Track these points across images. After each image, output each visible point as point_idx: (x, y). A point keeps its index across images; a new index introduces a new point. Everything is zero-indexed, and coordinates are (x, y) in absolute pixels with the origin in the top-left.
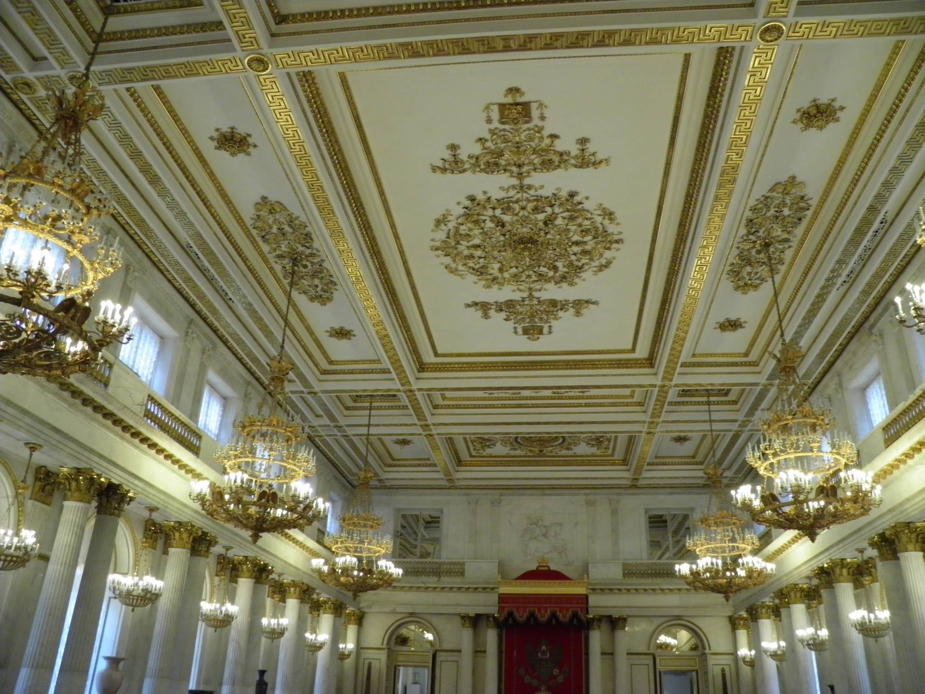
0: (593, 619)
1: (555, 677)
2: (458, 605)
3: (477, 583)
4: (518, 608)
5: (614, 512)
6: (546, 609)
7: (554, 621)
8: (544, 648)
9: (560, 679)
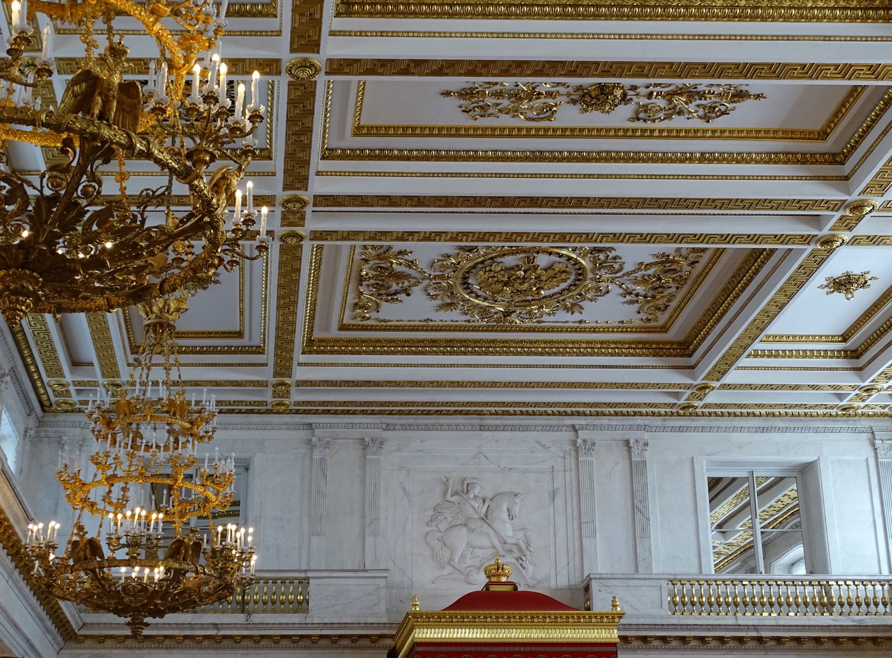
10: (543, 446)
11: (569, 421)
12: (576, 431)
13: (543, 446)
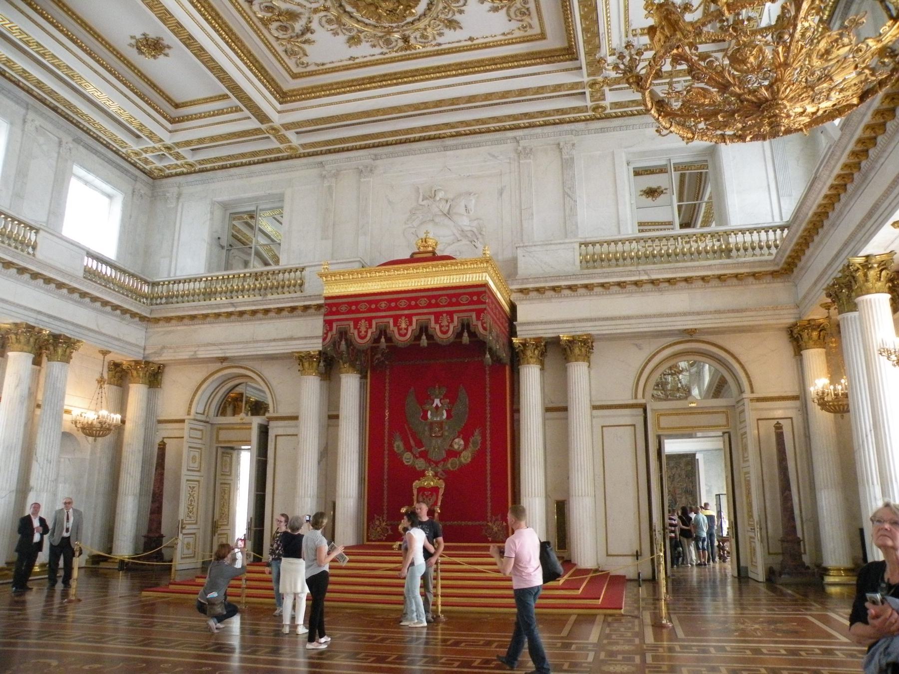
0: (524, 344)
2: (292, 339)
4: (356, 321)
5: (567, 164)
6: (409, 317)
7: (424, 341)
8: (437, 402)
9: (466, 457)
10: (493, 156)
11: (510, 134)
12: (518, 142)
13: (493, 156)
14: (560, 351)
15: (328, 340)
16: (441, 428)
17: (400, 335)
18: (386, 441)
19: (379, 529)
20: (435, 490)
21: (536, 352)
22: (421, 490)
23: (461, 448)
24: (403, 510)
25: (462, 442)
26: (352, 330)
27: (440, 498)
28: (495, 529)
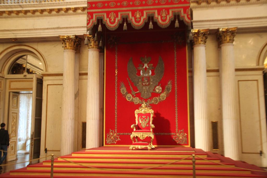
0: (198, 33)
1: (158, 95)
3: (76, 3)
4: (108, 13)
6: (142, 11)
7: (151, 26)
8: (146, 65)
9: (163, 96)
14: (218, 37)
15: (90, 24)
16: (149, 80)
17: (136, 21)
18: (116, 88)
19: (112, 137)
20: (149, 115)
21: (204, 38)
22: (140, 115)
23: (160, 91)
24: (132, 126)
25: (161, 88)
26: (106, 19)
27: (151, 119)
28: (181, 138)
